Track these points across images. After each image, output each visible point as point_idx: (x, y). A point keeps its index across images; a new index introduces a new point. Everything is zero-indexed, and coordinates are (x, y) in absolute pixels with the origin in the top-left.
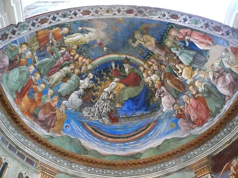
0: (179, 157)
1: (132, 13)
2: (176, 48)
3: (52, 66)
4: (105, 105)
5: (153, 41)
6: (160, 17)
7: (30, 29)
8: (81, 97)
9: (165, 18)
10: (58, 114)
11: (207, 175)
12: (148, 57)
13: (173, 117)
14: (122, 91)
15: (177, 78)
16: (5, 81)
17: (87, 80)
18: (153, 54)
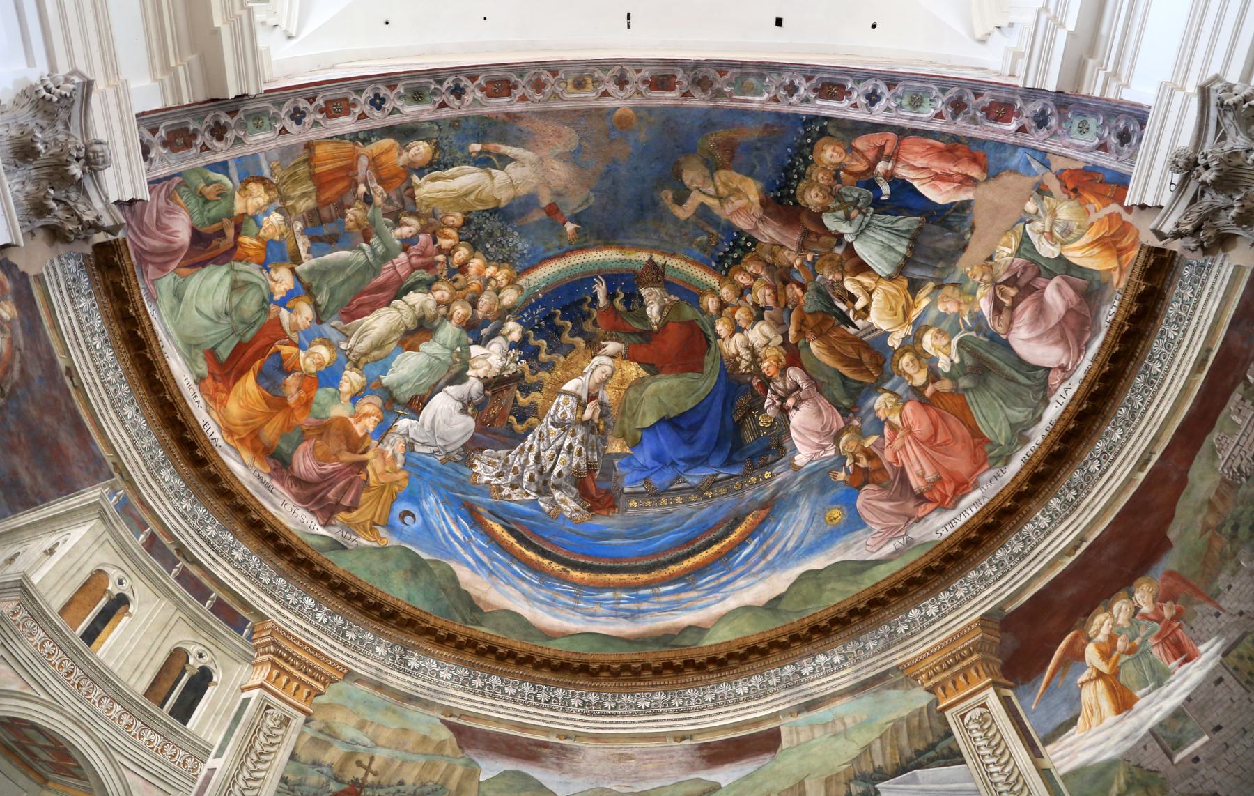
0: (862, 632)
1: (672, 89)
2: (841, 213)
3: (363, 281)
4: (565, 446)
5: (752, 191)
6: (775, 99)
7: (284, 131)
8: (470, 409)
9: (795, 98)
10: (375, 468)
11: (982, 695)
12: (735, 256)
13: (836, 484)
14: (636, 390)
15: (852, 330)
16: (166, 300)
17: (497, 345)
18: (755, 242)
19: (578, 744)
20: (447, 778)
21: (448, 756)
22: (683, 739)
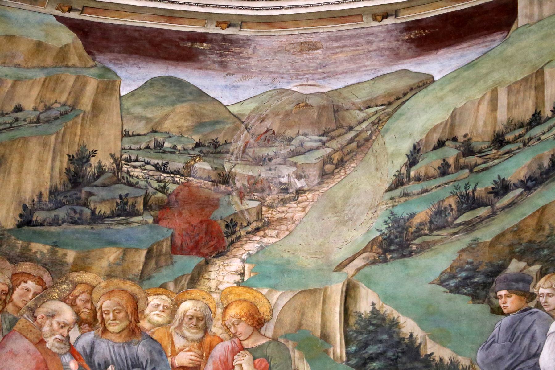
19: (245, 32)
20: (78, 95)
21: (74, 66)
22: (385, 16)
